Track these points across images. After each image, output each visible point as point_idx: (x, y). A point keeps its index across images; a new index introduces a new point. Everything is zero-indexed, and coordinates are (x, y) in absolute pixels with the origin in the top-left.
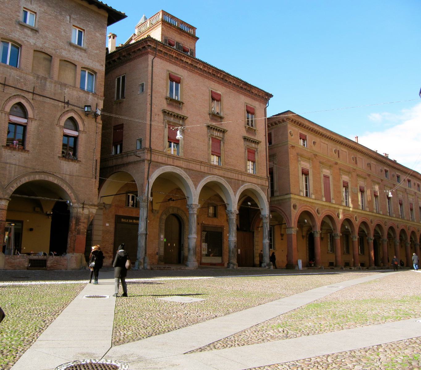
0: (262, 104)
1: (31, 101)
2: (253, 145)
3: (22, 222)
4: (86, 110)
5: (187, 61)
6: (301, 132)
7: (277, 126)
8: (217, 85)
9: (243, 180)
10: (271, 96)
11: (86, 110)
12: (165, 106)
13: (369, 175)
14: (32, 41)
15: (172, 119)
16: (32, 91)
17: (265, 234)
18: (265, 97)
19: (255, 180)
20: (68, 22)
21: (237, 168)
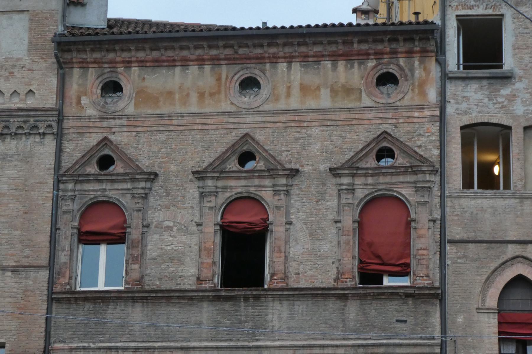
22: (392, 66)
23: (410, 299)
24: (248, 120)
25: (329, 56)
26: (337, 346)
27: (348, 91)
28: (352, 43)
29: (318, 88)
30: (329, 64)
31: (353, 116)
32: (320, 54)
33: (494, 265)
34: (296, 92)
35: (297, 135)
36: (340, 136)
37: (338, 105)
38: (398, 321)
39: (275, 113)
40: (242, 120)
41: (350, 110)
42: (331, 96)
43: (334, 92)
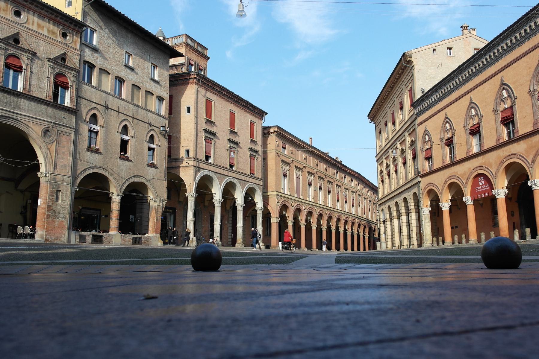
0: (260, 120)
1: (131, 122)
2: (254, 154)
3: (100, 210)
4: (161, 129)
5: (217, 89)
6: (283, 142)
7: (266, 136)
8: (233, 106)
9: (248, 181)
10: (266, 114)
11: (161, 129)
12: (250, 145)
13: (326, 176)
14: (130, 77)
15: (208, 135)
16: (132, 116)
17: (260, 222)
18: (261, 114)
19: (254, 181)
20: (149, 61)
21: (244, 172)
22: (67, 31)
23: (68, 111)
24: (18, 27)
25: (48, 17)
26: (45, 121)
27: (53, 33)
28: (58, 17)
29: (43, 27)
30: (47, 20)
31: (54, 42)
32: (46, 15)
33: (89, 108)
34: (35, 24)
35: (35, 41)
36: (50, 47)
37: (49, 36)
38: (63, 118)
39: (29, 29)
40: (16, 26)
41: (54, 40)
42: (47, 32)
43: (49, 31)
